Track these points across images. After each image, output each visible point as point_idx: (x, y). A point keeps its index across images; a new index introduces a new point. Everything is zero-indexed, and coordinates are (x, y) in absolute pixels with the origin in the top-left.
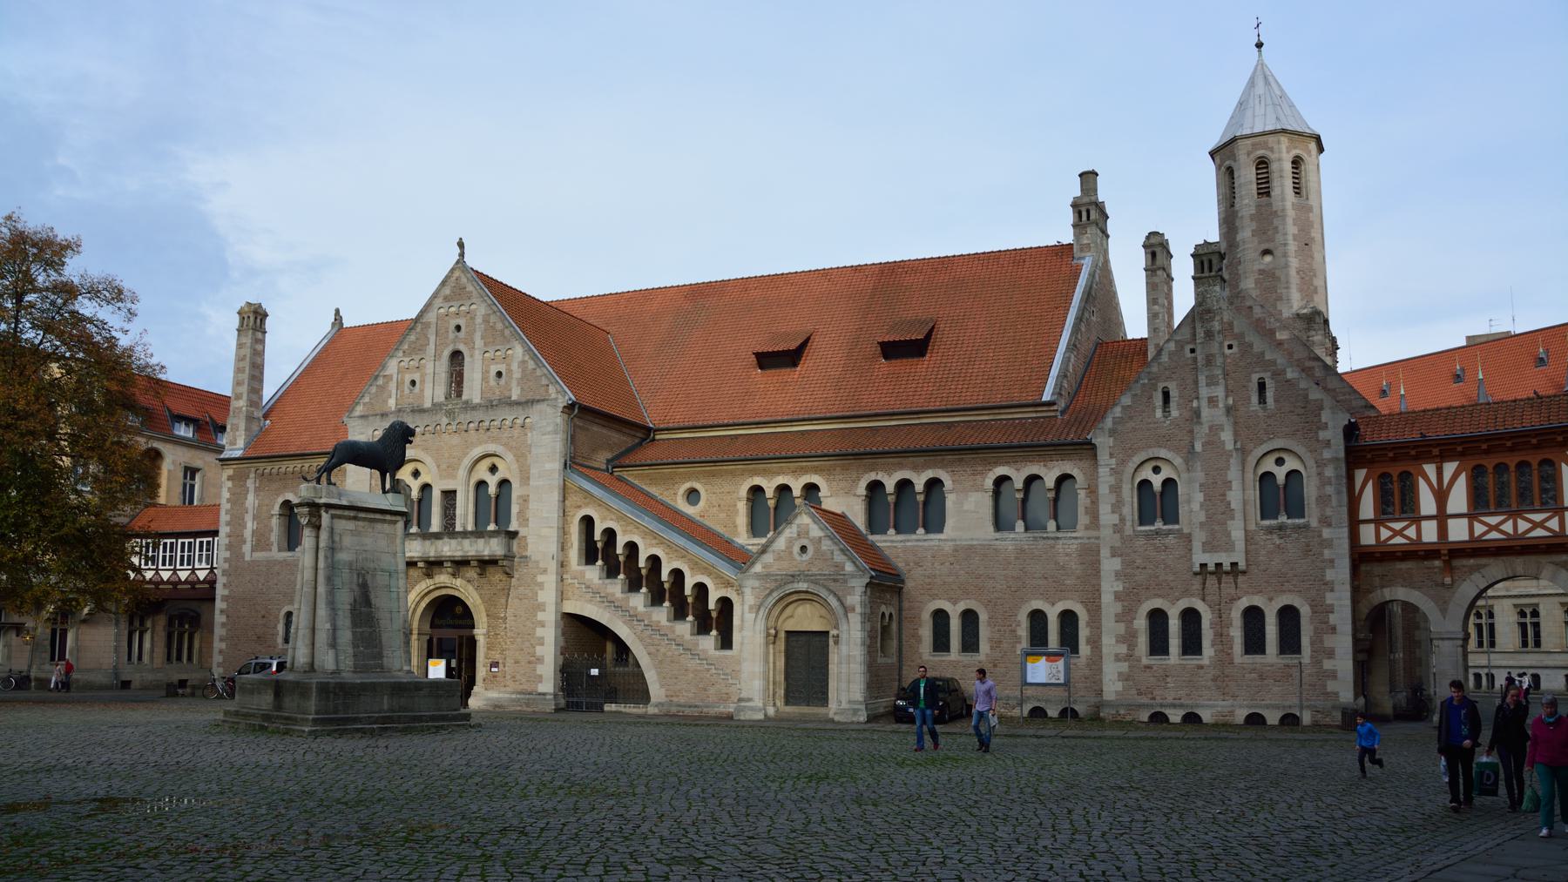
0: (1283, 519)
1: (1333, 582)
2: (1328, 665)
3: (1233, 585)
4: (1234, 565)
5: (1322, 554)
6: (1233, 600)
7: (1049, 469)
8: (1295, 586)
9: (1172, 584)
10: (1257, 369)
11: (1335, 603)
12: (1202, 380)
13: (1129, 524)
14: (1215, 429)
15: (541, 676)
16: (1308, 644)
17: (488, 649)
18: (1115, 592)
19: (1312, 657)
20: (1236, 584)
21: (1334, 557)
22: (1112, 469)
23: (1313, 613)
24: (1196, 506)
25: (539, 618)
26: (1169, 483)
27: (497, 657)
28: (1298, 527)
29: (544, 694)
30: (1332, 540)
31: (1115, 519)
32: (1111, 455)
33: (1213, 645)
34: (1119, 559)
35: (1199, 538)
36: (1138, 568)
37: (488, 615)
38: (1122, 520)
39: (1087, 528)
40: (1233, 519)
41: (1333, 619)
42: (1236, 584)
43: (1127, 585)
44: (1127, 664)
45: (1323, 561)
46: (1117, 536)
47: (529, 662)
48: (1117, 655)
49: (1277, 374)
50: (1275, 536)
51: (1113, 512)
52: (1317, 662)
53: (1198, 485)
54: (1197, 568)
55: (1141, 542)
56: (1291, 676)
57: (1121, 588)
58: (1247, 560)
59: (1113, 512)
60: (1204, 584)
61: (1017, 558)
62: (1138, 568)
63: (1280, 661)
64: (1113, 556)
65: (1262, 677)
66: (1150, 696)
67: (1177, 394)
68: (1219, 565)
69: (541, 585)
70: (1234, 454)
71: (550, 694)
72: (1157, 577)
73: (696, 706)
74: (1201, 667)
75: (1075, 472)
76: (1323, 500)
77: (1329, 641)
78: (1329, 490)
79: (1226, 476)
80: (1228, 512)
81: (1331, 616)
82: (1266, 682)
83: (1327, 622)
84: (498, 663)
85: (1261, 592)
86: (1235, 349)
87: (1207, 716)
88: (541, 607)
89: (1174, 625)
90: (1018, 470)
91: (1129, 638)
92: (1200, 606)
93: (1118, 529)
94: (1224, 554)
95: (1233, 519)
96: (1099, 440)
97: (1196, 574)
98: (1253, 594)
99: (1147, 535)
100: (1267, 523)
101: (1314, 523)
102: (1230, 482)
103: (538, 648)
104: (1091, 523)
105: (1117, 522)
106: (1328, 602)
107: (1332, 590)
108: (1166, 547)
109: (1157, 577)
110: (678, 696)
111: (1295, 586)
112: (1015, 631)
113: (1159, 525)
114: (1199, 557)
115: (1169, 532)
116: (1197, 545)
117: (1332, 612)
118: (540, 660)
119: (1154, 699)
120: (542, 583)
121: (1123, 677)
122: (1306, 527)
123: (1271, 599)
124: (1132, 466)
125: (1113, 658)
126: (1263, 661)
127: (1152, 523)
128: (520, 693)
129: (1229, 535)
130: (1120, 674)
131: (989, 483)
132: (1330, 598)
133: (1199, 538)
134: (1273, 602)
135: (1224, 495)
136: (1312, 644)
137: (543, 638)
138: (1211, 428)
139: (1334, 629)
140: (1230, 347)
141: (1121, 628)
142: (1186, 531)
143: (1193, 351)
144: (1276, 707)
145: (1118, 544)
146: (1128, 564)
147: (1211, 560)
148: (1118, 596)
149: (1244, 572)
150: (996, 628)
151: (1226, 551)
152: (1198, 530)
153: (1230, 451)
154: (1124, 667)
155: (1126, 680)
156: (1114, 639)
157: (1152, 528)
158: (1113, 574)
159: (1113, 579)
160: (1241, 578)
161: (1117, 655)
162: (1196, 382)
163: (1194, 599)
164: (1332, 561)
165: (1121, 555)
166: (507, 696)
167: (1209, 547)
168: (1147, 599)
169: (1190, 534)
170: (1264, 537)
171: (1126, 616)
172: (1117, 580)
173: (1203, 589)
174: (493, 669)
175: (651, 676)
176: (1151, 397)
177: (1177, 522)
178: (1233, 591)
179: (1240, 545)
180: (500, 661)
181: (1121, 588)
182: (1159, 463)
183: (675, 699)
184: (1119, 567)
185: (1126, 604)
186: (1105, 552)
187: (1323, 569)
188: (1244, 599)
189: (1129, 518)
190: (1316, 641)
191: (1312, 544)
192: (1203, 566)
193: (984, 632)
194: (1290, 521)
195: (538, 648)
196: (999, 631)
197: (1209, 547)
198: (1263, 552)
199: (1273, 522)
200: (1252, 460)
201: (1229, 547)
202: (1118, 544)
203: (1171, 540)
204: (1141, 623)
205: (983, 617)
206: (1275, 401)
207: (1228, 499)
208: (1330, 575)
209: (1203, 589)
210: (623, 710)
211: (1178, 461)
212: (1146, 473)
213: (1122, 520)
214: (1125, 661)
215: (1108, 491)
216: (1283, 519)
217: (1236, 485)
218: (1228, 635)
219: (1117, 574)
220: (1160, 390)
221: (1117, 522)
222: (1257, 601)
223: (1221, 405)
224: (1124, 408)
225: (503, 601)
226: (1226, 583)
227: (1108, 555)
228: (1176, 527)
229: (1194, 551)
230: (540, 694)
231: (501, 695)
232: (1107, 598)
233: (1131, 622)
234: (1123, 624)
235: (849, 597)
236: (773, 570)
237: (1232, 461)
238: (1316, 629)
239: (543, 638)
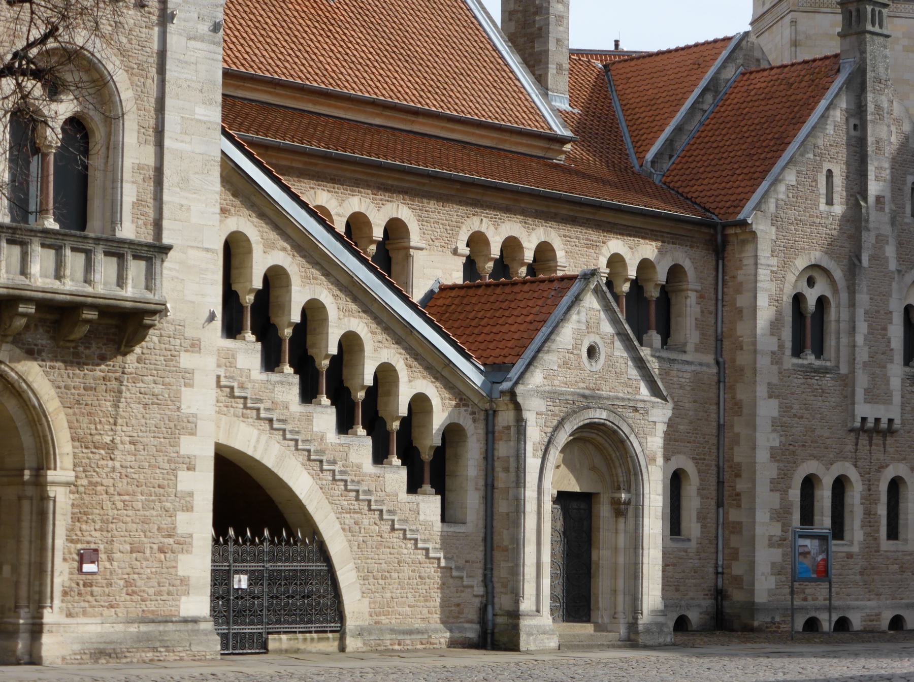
3: (882, 449)
4: (891, 421)
6: (882, 467)
13: (788, 352)
14: (881, 240)
15: (184, 581)
17: (76, 518)
18: (772, 448)
20: (884, 447)
22: (772, 272)
25: (183, 451)
27: (94, 537)
29: (195, 621)
33: (862, 527)
36: (795, 416)
37: (73, 439)
38: (781, 346)
39: (697, 350)
40: (892, 362)
42: (884, 447)
44: (780, 550)
46: (775, 367)
47: (161, 550)
48: (770, 538)
54: (858, 424)
55: (798, 380)
58: (902, 420)
59: (772, 334)
60: (857, 444)
62: (795, 416)
64: (770, 397)
66: (802, 596)
68: (877, 420)
69: (187, 378)
71: (205, 620)
73: (419, 632)
74: (850, 556)
75: (687, 265)
80: (888, 351)
84: (96, 551)
85: (904, 459)
87: (857, 621)
88: (189, 426)
89: (824, 496)
90: (631, 248)
91: (781, 515)
92: (853, 474)
95: (892, 361)
96: (761, 227)
97: (852, 430)
102: (891, 313)
103: (181, 517)
104: (701, 343)
105: (775, 349)
109: (813, 431)
110: (387, 614)
113: (810, 359)
114: (864, 410)
115: (825, 371)
118: (184, 544)
119: (805, 599)
120: (192, 372)
121: (777, 570)
125: (766, 542)
128: (144, 621)
129: (888, 383)
130: (773, 564)
133: (862, 381)
135: (885, 329)
137: (191, 494)
145: (775, 380)
146: (785, 409)
148: (774, 455)
153: (892, 272)
155: (779, 574)
156: (768, 515)
158: (770, 423)
159: (770, 429)
160: (889, 441)
161: (770, 538)
165: (777, 397)
166: (120, 628)
168: (803, 460)
169: (846, 376)
171: (780, 484)
172: (774, 431)
173: (857, 450)
174: (87, 567)
175: (346, 576)
176: (816, 181)
179: (897, 398)
180: (102, 547)
183: (384, 620)
184: (775, 413)
185: (782, 465)
192: (864, 420)
195: (181, 517)
197: (872, 397)
202: (775, 380)
203: (828, 381)
204: (795, 494)
209: (857, 450)
210: (302, 646)
211: (838, 274)
214: (779, 546)
218: (875, 514)
220: (824, 172)
221: (775, 349)
223: (887, 210)
224: (789, 188)
225: (108, 406)
227: (765, 395)
230: (185, 621)
231: (107, 628)
235: (649, 439)
236: (558, 383)
237: (895, 285)
239: (191, 494)
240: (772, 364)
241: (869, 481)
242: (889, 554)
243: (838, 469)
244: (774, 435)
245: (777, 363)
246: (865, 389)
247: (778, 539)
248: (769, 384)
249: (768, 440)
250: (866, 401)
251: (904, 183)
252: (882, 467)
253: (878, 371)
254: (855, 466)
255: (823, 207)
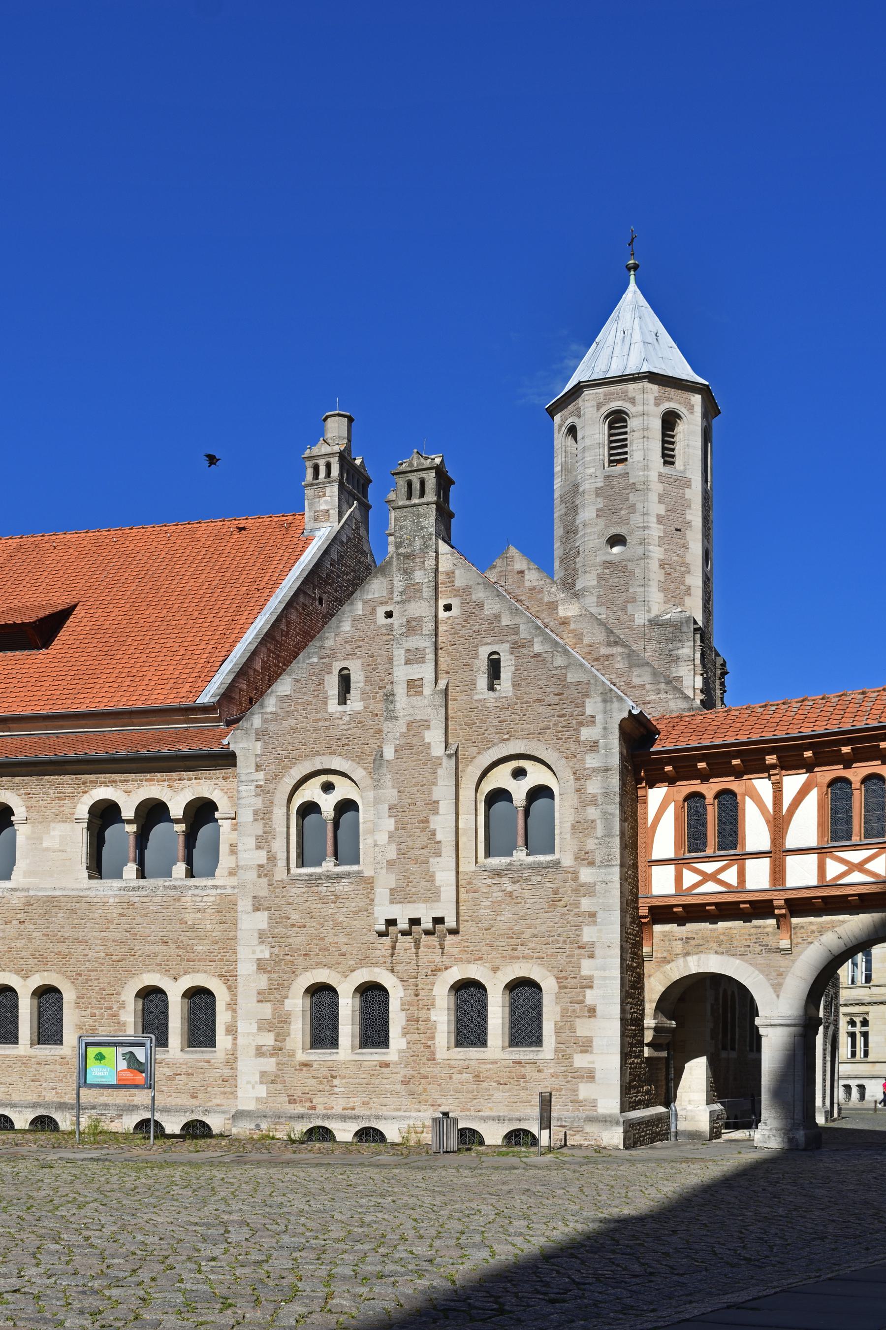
0: (520, 855)
1: (592, 945)
2: (580, 1061)
4: (439, 921)
5: (577, 904)
6: (436, 971)
7: (176, 791)
8: (534, 950)
9: (344, 949)
10: (488, 640)
11: (596, 974)
12: (399, 655)
13: (281, 863)
16: (553, 1033)
19: (557, 1050)
20: (442, 947)
21: (597, 909)
23: (560, 988)
24: (382, 838)
26: (346, 806)
28: (538, 868)
30: (594, 884)
31: (261, 857)
32: (258, 767)
34: (266, 913)
35: (385, 882)
36: (293, 925)
38: (272, 858)
41: (591, 996)
42: (442, 947)
43: (276, 950)
45: (578, 915)
46: (264, 880)
49: (516, 647)
50: (505, 880)
51: (258, 848)
52: (563, 1056)
53: (386, 807)
56: (524, 1077)
57: (267, 956)
59: (258, 848)
60: (394, 948)
61: (121, 915)
62: (293, 925)
63: (507, 1056)
64: (257, 910)
65: (478, 1078)
67: (362, 678)
68: (415, 922)
70: (445, 760)
72: (323, 939)
76: (581, 827)
77: (584, 1027)
78: (593, 813)
79: (430, 793)
81: (588, 991)
82: (485, 1085)
83: (581, 1002)
85: (480, 959)
86: (455, 611)
87: (392, 1132)
90: (128, 792)
93: (263, 871)
94: (423, 905)
97: (381, 934)
98: (469, 962)
99: (311, 881)
100: (495, 862)
101: (567, 861)
105: (264, 861)
106: (585, 972)
107: (591, 956)
108: (337, 897)
109: (323, 939)
111: (534, 950)
112: (115, 1016)
113: (328, 866)
114: (384, 910)
116: (382, 893)
117: (591, 987)
122: (557, 863)
123: (495, 969)
124: (289, 782)
126: (482, 1056)
127: (319, 864)
131: (83, 810)
132: (587, 967)
134: (499, 973)
136: (558, 1031)
138: (409, 725)
139: (592, 1012)
140: (448, 608)
141: (266, 1011)
142: (368, 873)
143: (389, 615)
144: (499, 1119)
145: (264, 893)
147: (402, 914)
149: (454, 932)
150: (88, 1011)
151: (426, 900)
152: (384, 871)
154: (269, 1064)
156: (255, 1026)
157: (318, 870)
158: (256, 935)
162: (391, 660)
163: (377, 970)
164: (593, 915)
165: (268, 909)
167: (398, 895)
170: (488, 881)
173: (393, 954)
177: (357, 862)
178: (438, 959)
181: (267, 955)
182: (331, 778)
184: (264, 925)
185: (274, 976)
186: (245, 904)
187: (578, 926)
188: (455, 968)
189: (281, 856)
190: (565, 1027)
191: (561, 890)
192: (391, 922)
193: (70, 1018)
194: (531, 859)
196: (94, 1015)
198: (487, 903)
199: (505, 860)
200: (471, 773)
201: (433, 895)
205: (69, 996)
206: (514, 686)
207: (432, 826)
208: (588, 934)
209: (393, 954)
212: (311, 792)
213: (272, 858)
215: (251, 819)
216: (520, 855)
217: (446, 807)
219: (262, 937)
221: (264, 861)
222: (474, 972)
226: (427, 946)
227: (250, 908)
228: (355, 868)
229: (376, 902)
232: (246, 968)
233: (282, 1002)
234: (269, 1005)
238: (564, 1011)
240: (259, 876)
241: (417, 986)
242: (452, 1062)
243: (363, 976)
244: (263, 947)
245: (266, 875)
246: (391, 890)
247: (270, 1048)
248: (255, 897)
249: (254, 952)
250: (392, 902)
251: (476, 656)
252: (440, 970)
253: (413, 868)
254: (392, 971)
255: (333, 706)
